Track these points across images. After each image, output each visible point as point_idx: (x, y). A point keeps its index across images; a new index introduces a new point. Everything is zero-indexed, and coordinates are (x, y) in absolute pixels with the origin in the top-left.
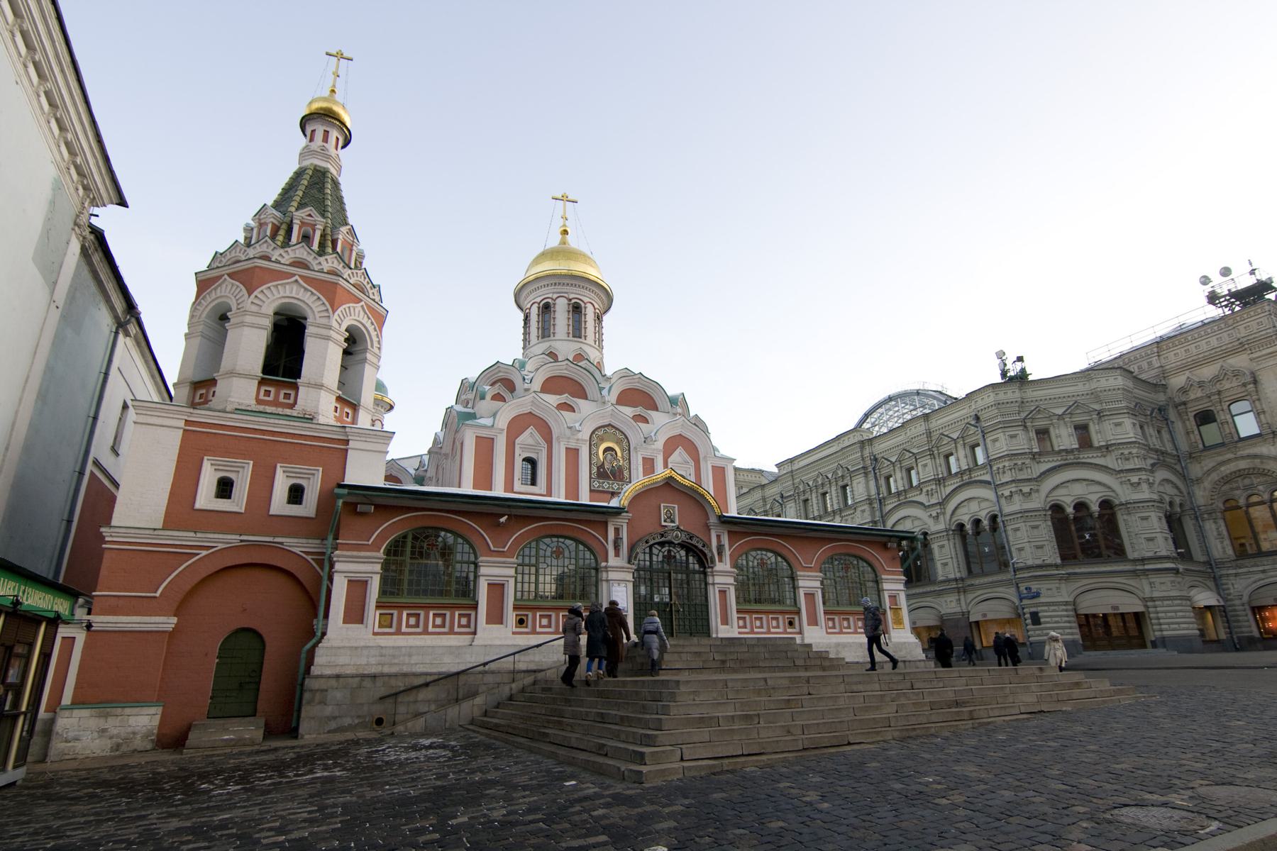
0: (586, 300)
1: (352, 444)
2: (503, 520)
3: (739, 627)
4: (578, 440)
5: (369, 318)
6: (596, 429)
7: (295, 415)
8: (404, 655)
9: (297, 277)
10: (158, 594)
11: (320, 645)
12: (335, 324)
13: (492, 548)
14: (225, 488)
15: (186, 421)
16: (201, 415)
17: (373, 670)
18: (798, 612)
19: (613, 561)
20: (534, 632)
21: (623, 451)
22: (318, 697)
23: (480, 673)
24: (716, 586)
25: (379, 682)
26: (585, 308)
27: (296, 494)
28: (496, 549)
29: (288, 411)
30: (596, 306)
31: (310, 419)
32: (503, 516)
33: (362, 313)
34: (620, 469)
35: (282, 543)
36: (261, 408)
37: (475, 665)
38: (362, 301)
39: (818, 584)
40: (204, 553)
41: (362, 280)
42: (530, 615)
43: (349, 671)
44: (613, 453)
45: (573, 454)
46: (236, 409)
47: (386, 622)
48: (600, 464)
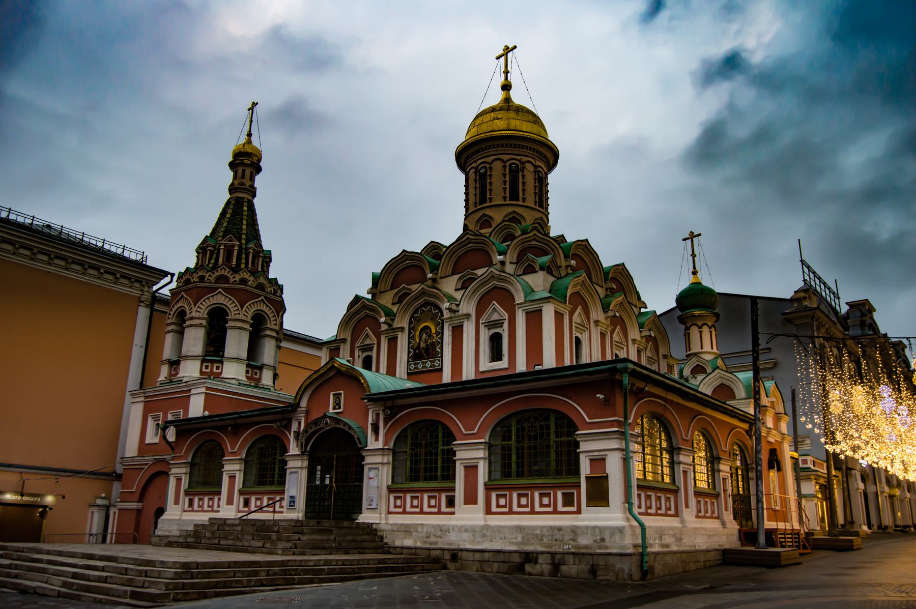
0: (489, 159)
1: (192, 393)
4: (393, 329)
6: (416, 312)
9: (183, 293)
12: (194, 314)
15: (146, 397)
16: (149, 391)
18: (453, 490)
19: (294, 449)
24: (368, 466)
26: (491, 168)
28: (232, 451)
30: (505, 157)
32: (228, 426)
34: (433, 345)
35: (165, 459)
38: (218, 288)
39: (481, 454)
40: (146, 467)
41: (223, 272)
44: (428, 331)
47: (191, 504)
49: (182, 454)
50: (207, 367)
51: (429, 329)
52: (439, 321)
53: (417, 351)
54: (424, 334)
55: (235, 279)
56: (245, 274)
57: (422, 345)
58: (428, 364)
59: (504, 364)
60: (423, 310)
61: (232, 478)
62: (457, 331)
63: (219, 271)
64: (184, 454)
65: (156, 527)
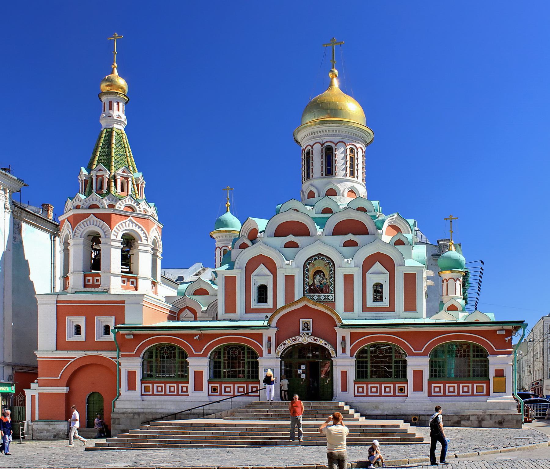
7: (100, 291)
10: (59, 378)
13: (194, 353)
17: (140, 411)
20: (221, 395)
21: (331, 270)
22: (117, 422)
23: (187, 414)
25: (141, 416)
29: (97, 290)
31: (106, 292)
33: (131, 224)
34: (327, 286)
36: (86, 290)
38: (129, 216)
40: (73, 360)
41: (130, 203)
42: (218, 385)
45: (289, 279)
46: (75, 292)
49: (134, 353)
50: (124, 282)
51: (322, 273)
52: (331, 268)
53: (312, 287)
54: (318, 276)
55: (140, 210)
56: (145, 205)
57: (317, 283)
58: (323, 298)
59: (386, 303)
61: (198, 375)
62: (348, 279)
63: (127, 201)
65: (114, 407)
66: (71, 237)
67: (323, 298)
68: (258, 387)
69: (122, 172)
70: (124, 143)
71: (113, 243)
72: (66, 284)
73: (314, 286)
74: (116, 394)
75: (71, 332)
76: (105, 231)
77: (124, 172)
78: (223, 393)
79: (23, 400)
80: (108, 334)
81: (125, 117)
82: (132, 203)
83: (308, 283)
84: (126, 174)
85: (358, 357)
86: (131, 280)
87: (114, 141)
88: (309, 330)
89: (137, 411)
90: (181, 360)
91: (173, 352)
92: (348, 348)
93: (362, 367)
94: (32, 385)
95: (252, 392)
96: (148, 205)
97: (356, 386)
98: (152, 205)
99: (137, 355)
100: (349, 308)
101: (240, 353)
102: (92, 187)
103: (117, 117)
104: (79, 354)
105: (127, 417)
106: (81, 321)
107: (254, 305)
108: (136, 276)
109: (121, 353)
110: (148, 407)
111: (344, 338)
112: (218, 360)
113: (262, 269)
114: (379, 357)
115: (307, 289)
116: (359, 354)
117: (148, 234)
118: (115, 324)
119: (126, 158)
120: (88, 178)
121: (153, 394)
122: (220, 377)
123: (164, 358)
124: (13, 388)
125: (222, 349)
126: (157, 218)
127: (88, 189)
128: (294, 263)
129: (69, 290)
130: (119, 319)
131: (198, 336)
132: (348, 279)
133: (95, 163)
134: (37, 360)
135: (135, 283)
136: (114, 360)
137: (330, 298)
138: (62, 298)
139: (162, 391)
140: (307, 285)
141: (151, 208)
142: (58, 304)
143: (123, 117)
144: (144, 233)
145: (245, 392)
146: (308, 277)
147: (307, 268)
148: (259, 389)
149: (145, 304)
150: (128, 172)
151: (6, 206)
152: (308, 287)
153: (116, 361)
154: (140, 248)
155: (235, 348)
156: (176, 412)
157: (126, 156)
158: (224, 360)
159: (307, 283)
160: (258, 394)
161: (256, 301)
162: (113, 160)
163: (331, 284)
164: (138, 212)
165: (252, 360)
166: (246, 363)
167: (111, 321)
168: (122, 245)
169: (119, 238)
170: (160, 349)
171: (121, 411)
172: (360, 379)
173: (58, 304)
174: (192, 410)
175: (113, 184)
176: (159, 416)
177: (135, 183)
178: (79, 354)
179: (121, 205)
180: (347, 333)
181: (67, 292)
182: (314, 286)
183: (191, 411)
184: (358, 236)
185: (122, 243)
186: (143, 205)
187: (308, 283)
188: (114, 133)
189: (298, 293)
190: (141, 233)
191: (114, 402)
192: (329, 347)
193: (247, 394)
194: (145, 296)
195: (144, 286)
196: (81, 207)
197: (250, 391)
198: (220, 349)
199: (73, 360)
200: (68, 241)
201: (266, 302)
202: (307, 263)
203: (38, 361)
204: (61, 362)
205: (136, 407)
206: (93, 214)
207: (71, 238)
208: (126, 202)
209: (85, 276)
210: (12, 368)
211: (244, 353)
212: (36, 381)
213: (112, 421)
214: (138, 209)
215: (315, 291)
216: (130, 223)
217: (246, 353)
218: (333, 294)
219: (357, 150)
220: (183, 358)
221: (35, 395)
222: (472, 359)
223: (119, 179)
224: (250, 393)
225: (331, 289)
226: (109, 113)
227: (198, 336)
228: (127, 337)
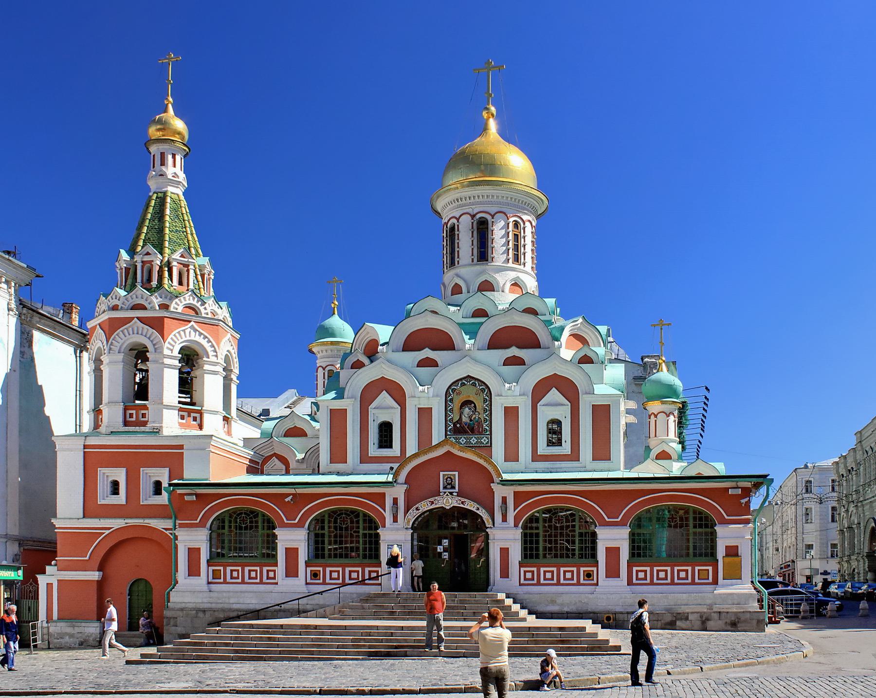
2: (288, 499)
3: (525, 579)
5: (201, 334)
8: (225, 598)
11: (173, 590)
13: (286, 521)
14: (115, 490)
20: (324, 583)
21: (485, 401)
22: (172, 622)
25: (208, 614)
27: (158, 488)
29: (142, 429)
31: (157, 432)
33: (193, 333)
34: (479, 423)
36: (127, 429)
37: (269, 606)
38: (190, 321)
40: (107, 532)
41: (191, 301)
42: (321, 569)
43: (191, 606)
45: (425, 414)
46: (112, 432)
48: (454, 422)
50: (182, 418)
51: (473, 405)
52: (486, 397)
53: (458, 426)
54: (467, 409)
55: (206, 311)
56: (213, 304)
57: (465, 419)
58: (474, 440)
59: (566, 448)
60: (464, 383)
61: (291, 553)
62: (511, 413)
63: (187, 298)
64: (200, 521)
65: (169, 601)
66: (105, 352)
67: (474, 440)
68: (377, 572)
69: (180, 257)
70: (182, 214)
71: (167, 361)
72: (98, 421)
73: (460, 424)
74: (171, 582)
75: (105, 490)
76: (154, 342)
77: (182, 256)
78: (328, 580)
79: (35, 591)
80: (160, 494)
81: (184, 175)
82: (195, 302)
83: (452, 418)
84: (186, 260)
85: (525, 527)
86: (193, 415)
87: (168, 212)
88: (453, 487)
89: (202, 606)
90: (266, 532)
91: (254, 520)
92: (511, 514)
93: (531, 542)
94: (48, 568)
95: (370, 579)
96: (217, 305)
97: (522, 569)
98: (224, 304)
99: (202, 525)
100: (512, 455)
101: (352, 522)
102: (136, 279)
103: (173, 176)
104: (117, 523)
105: (187, 615)
106: (120, 475)
107: (374, 450)
108: (200, 408)
109: (178, 522)
110: (218, 601)
111: (504, 500)
112: (321, 532)
113: (384, 398)
114: (556, 528)
115: (450, 427)
116: (526, 523)
117: (218, 347)
118: (170, 479)
119: (186, 237)
120: (131, 265)
121: (225, 582)
122: (323, 557)
123: (241, 528)
124: (21, 572)
125: (327, 516)
126: (231, 324)
127: (129, 281)
128: (431, 390)
129: (102, 429)
130: (176, 470)
131: (292, 496)
132: (511, 413)
133: (141, 243)
134: (56, 532)
135: (198, 419)
136: (167, 532)
137: (485, 440)
138: (92, 441)
139: (238, 578)
140: (450, 422)
141: (222, 308)
142: (86, 450)
143: (182, 177)
144: (213, 346)
145: (360, 579)
146: (452, 410)
147: (450, 397)
148: (380, 574)
149: (213, 451)
150: (188, 256)
151: (9, 306)
152: (452, 426)
153: (171, 534)
154: (207, 367)
155: (345, 514)
156: (258, 607)
157: (185, 234)
158: (330, 532)
159: (450, 419)
160: (379, 582)
161: (377, 445)
162: (167, 238)
163: (486, 420)
164: (204, 315)
165: (371, 532)
166: (361, 536)
167: (163, 475)
168: (179, 363)
169: (176, 353)
170: (235, 515)
171: (179, 606)
172: (529, 561)
173: (86, 450)
174: (282, 605)
175: (166, 274)
176: (235, 614)
177: (198, 273)
178: (117, 523)
179: (178, 305)
180: (508, 492)
181: (100, 433)
182: (460, 424)
183: (281, 607)
184: (525, 350)
185: (179, 360)
186: (211, 305)
187: (452, 418)
188: (168, 200)
189: (438, 433)
190: (207, 346)
191: (169, 593)
192: (482, 513)
193: (363, 582)
194: (213, 438)
195: (213, 424)
196: (120, 307)
197: (367, 577)
198: (324, 516)
199: (107, 532)
200: (101, 357)
201: (391, 447)
202: (451, 390)
203: (57, 534)
204: (90, 536)
205: (200, 601)
206: (137, 318)
207: (105, 354)
208: (185, 301)
209: (126, 409)
210: (19, 544)
211: (358, 522)
212: (53, 562)
213: (165, 621)
214: (203, 311)
215: (463, 431)
216: (192, 331)
217: (361, 522)
218: (487, 435)
219: (524, 224)
220: (269, 528)
221: (52, 584)
222: (692, 530)
223: (175, 266)
224: (367, 579)
225: (486, 427)
226: (161, 170)
227: (292, 496)
228: (186, 498)
